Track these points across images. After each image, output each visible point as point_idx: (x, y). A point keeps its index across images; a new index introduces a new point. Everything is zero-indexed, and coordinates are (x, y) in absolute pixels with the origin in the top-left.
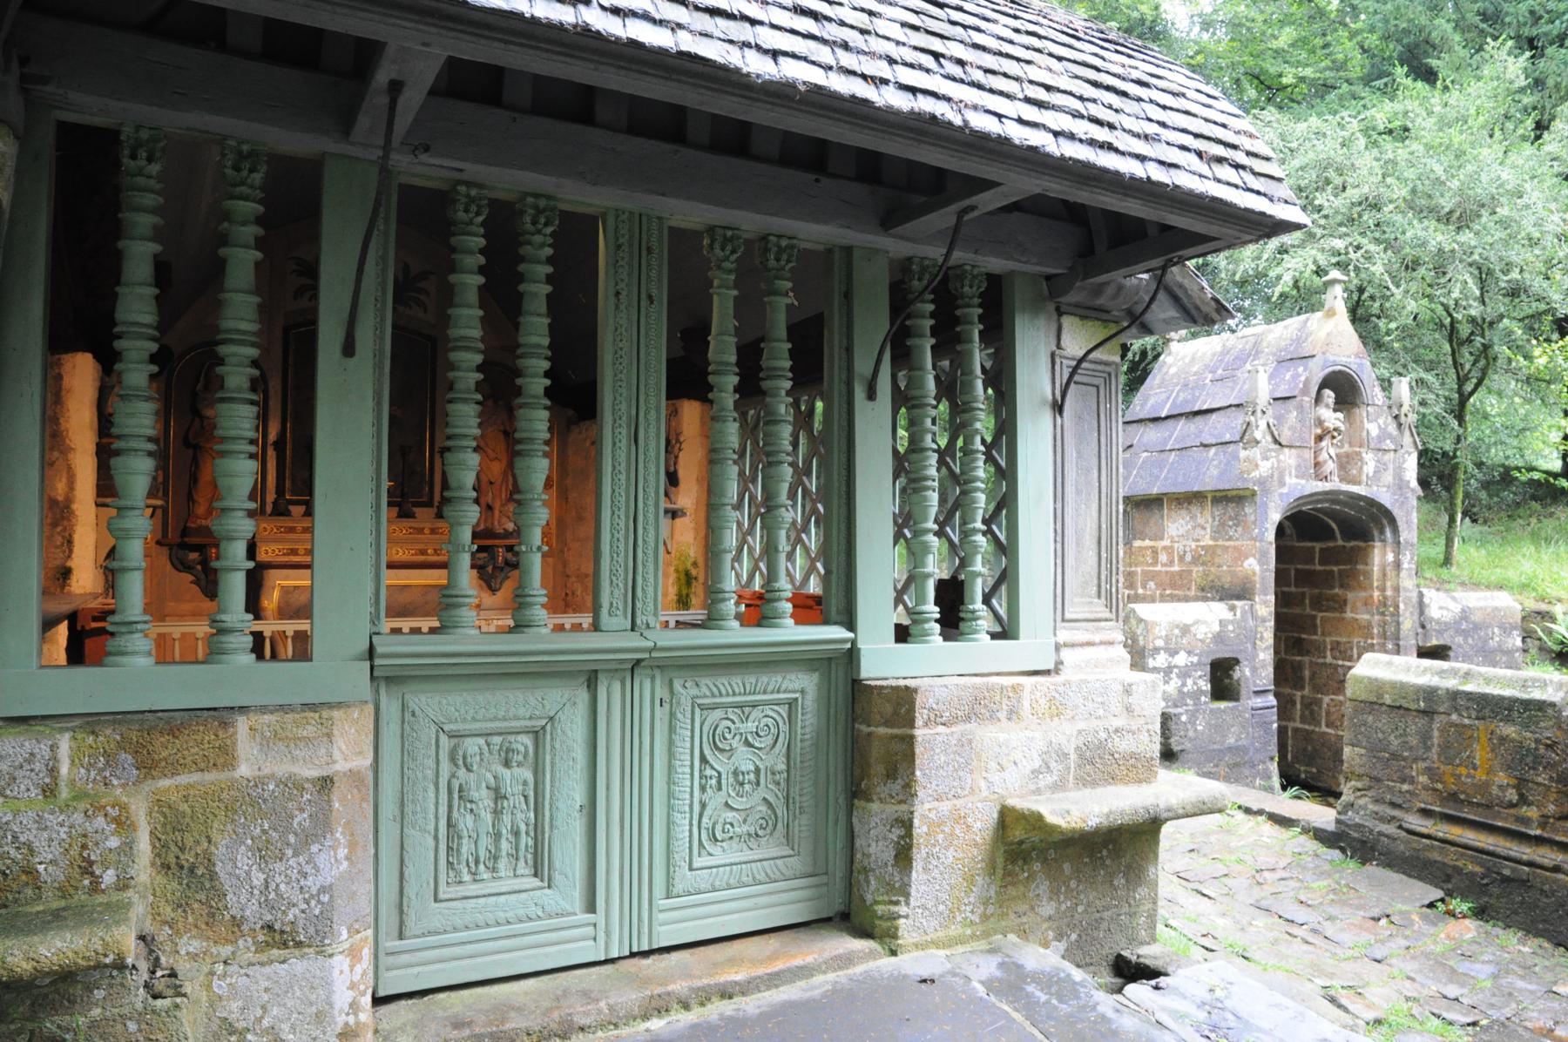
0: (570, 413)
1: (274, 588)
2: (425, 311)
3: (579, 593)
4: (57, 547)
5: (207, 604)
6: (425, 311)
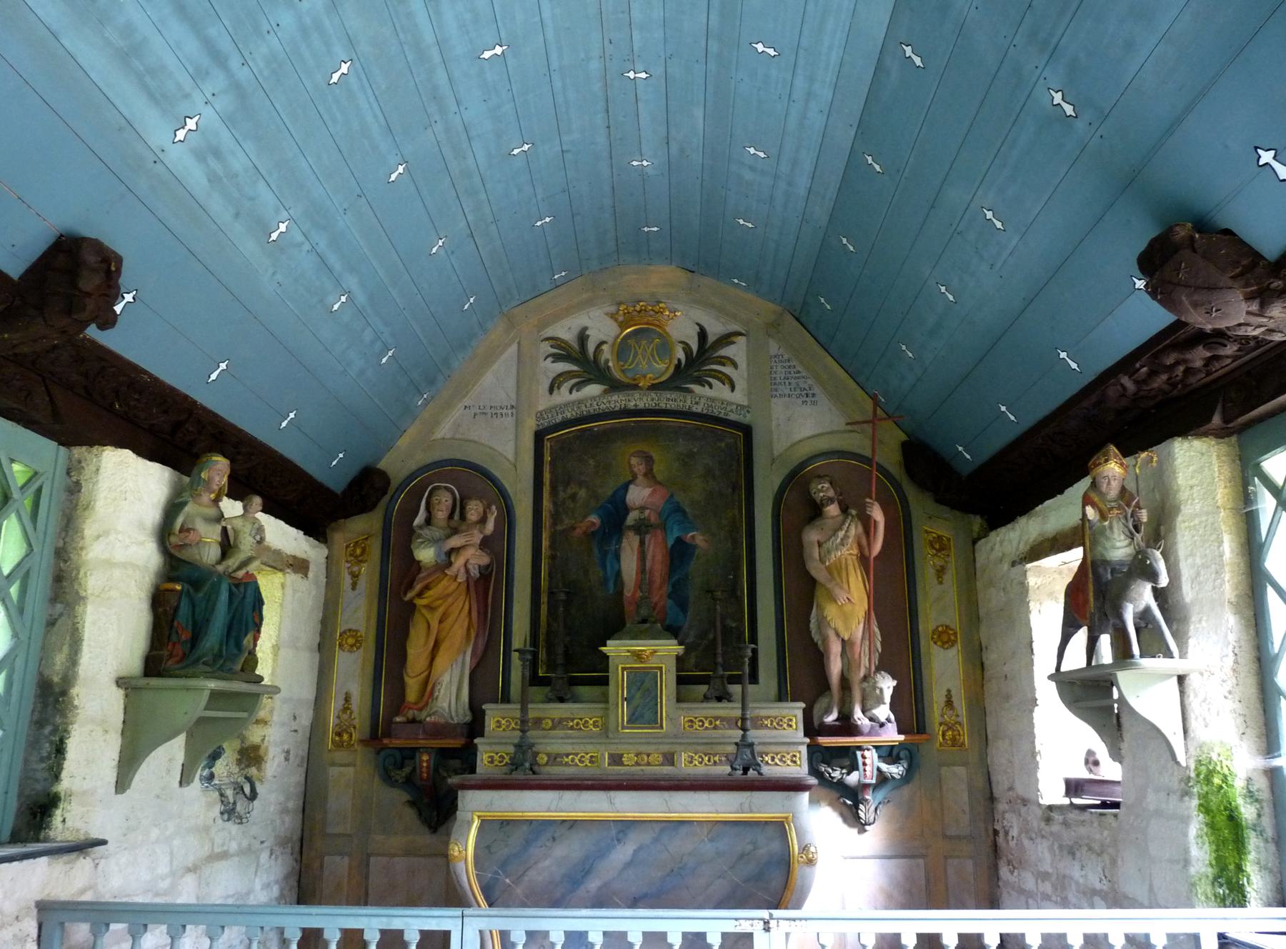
0: (977, 522)
1: (470, 823)
2: (733, 388)
3: (1014, 832)
4: (42, 760)
5: (425, 839)
6: (733, 388)
